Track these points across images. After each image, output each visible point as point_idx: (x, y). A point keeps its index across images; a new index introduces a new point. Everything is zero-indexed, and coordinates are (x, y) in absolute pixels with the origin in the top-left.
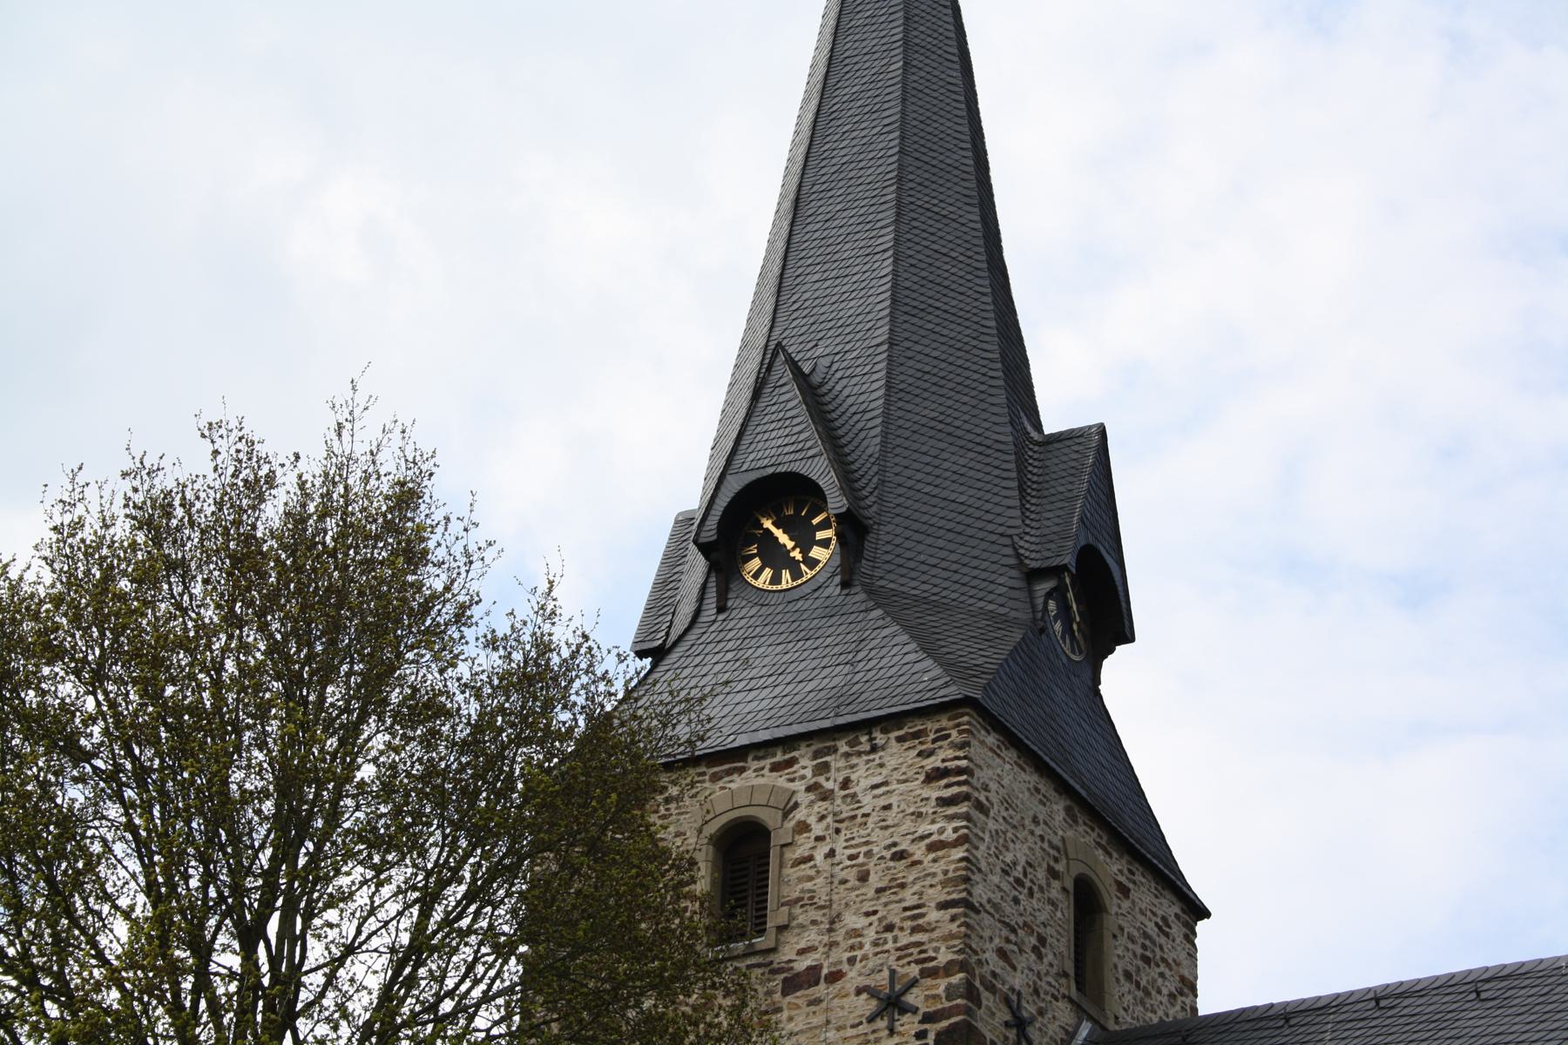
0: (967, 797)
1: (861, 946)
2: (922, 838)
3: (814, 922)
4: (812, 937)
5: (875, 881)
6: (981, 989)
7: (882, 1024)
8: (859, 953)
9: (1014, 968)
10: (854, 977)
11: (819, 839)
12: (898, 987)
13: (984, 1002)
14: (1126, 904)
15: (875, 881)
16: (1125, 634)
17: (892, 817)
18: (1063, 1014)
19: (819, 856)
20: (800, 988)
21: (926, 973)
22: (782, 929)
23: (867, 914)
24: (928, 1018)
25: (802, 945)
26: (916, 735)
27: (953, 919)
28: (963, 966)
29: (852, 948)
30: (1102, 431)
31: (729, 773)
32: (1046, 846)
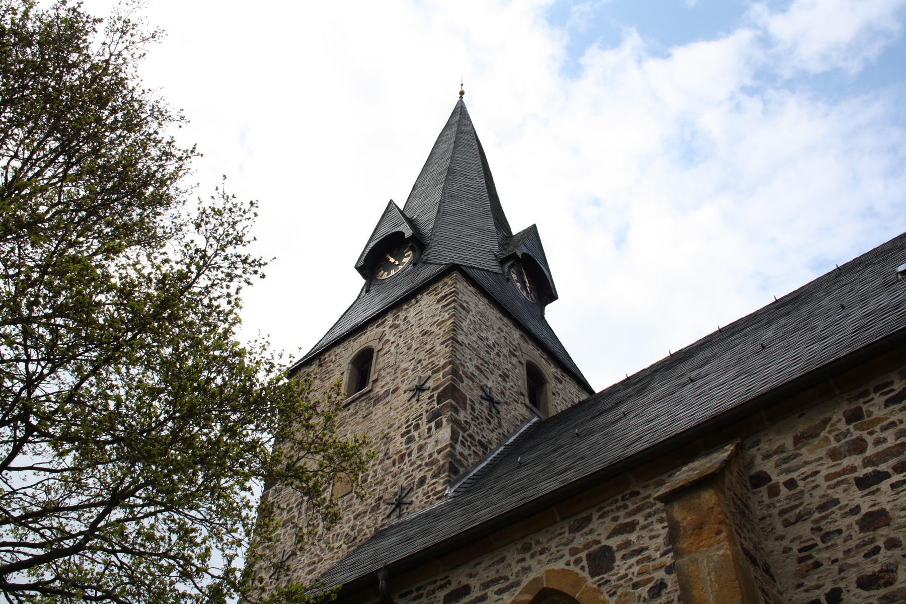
0: (454, 301)
1: (407, 373)
2: (435, 323)
3: (388, 373)
4: (388, 379)
5: (414, 347)
6: (463, 376)
7: (414, 400)
8: (406, 377)
9: (488, 379)
10: (404, 387)
11: (392, 343)
12: (422, 383)
13: (465, 382)
14: (560, 386)
15: (414, 347)
16: (552, 296)
17: (422, 322)
18: (521, 410)
19: (392, 349)
20: (379, 402)
21: (433, 373)
22: (375, 381)
23: (410, 360)
24: (434, 390)
25: (383, 384)
26: (433, 290)
27: (446, 346)
28: (450, 363)
29: (403, 376)
30: (534, 226)
31: (360, 336)
32: (508, 342)
